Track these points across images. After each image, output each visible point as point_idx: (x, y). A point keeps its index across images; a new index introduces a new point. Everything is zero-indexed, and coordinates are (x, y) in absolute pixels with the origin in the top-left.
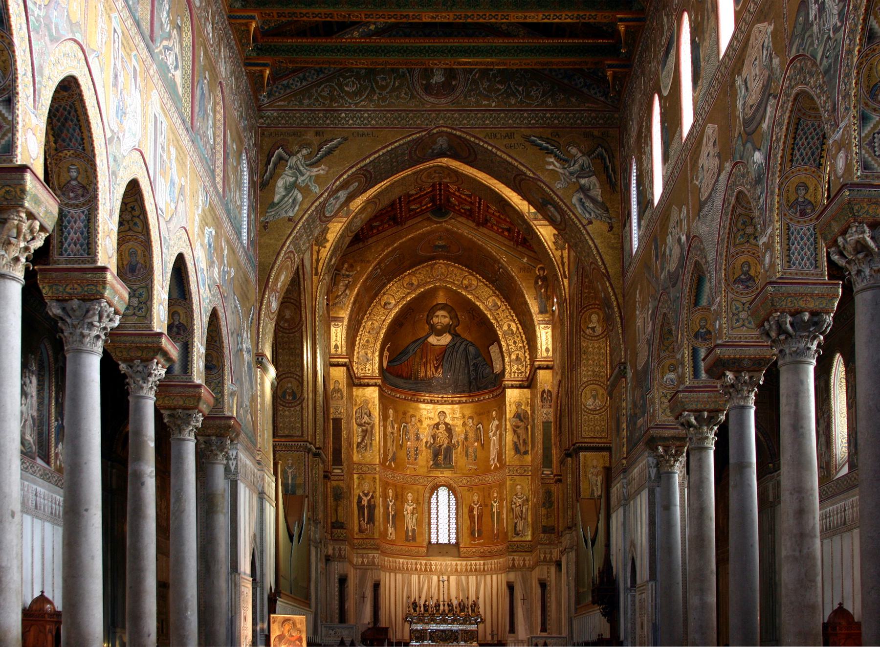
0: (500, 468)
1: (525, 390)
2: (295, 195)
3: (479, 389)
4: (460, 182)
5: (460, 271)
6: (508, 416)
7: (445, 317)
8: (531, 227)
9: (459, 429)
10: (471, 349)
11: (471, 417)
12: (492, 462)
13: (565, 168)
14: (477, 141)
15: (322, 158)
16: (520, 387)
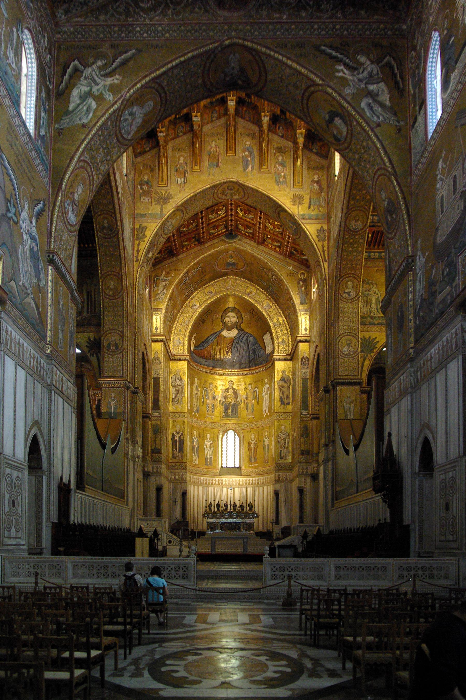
0: (270, 415)
1: (288, 362)
2: (89, 103)
3: (256, 365)
4: (246, 198)
5: (244, 283)
6: (276, 379)
7: (234, 317)
8: (299, 225)
9: (242, 392)
10: (251, 339)
11: (250, 384)
12: (264, 412)
13: (355, 75)
14: (268, 51)
15: (116, 68)
16: (285, 360)
